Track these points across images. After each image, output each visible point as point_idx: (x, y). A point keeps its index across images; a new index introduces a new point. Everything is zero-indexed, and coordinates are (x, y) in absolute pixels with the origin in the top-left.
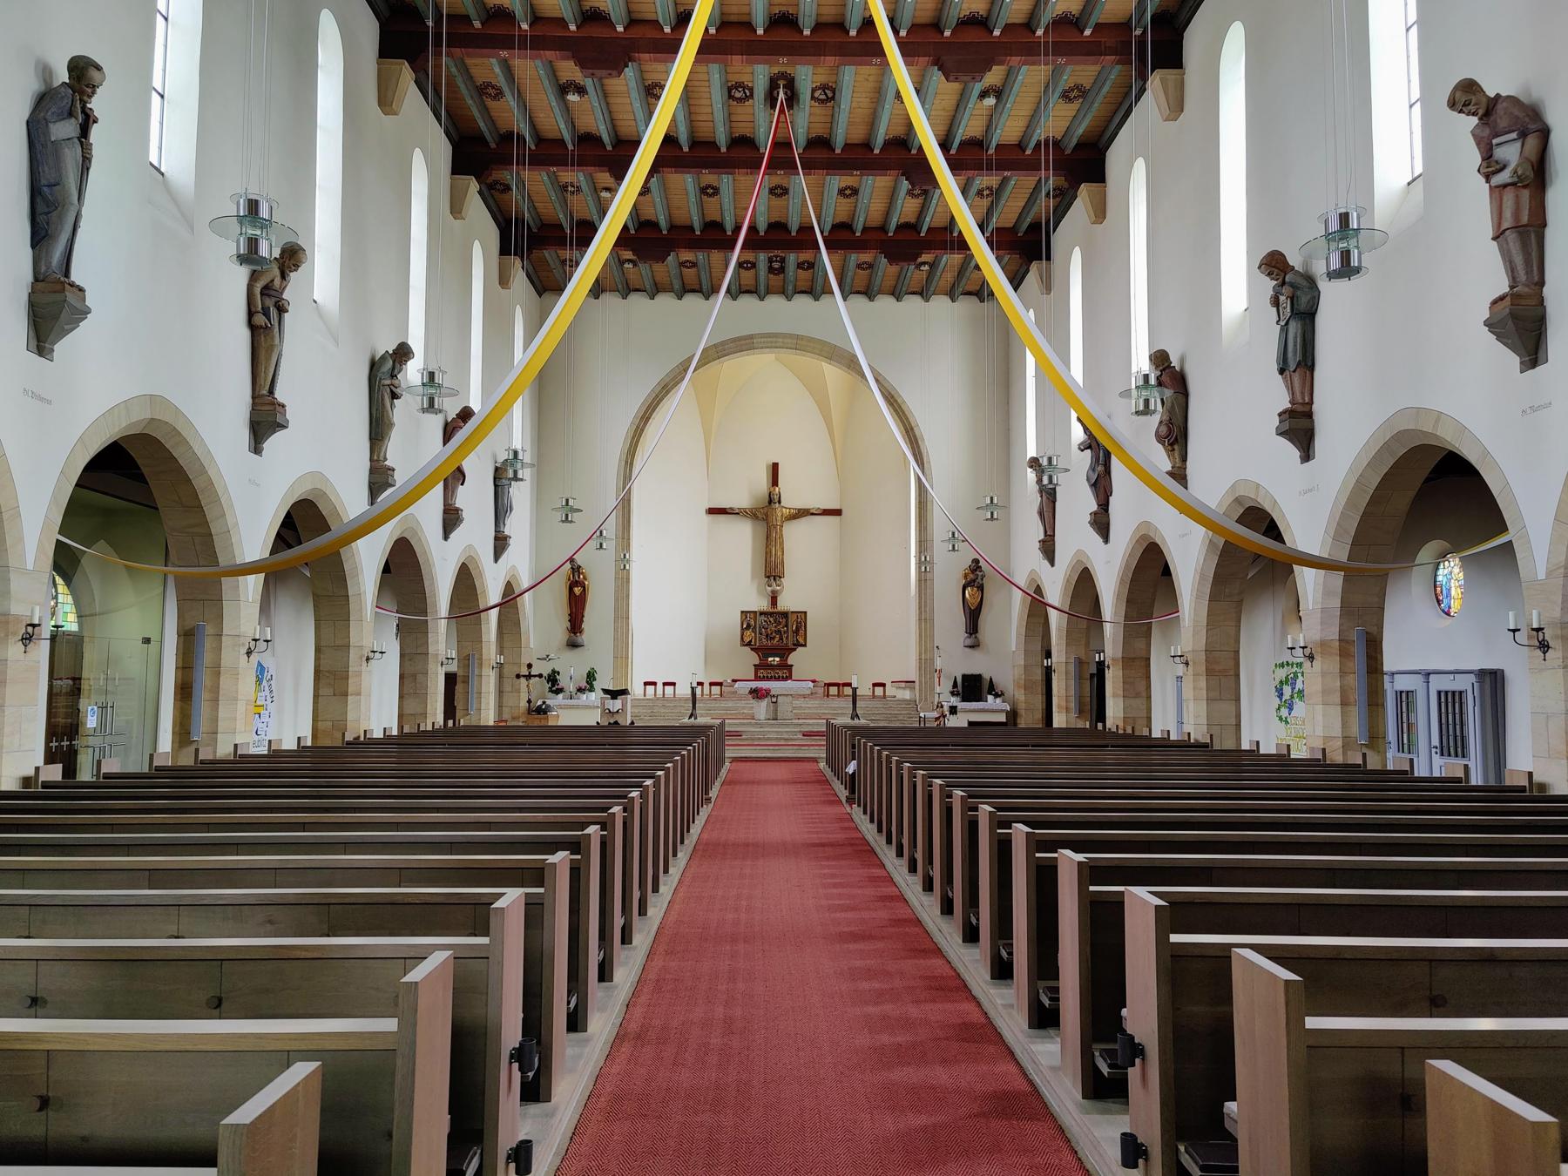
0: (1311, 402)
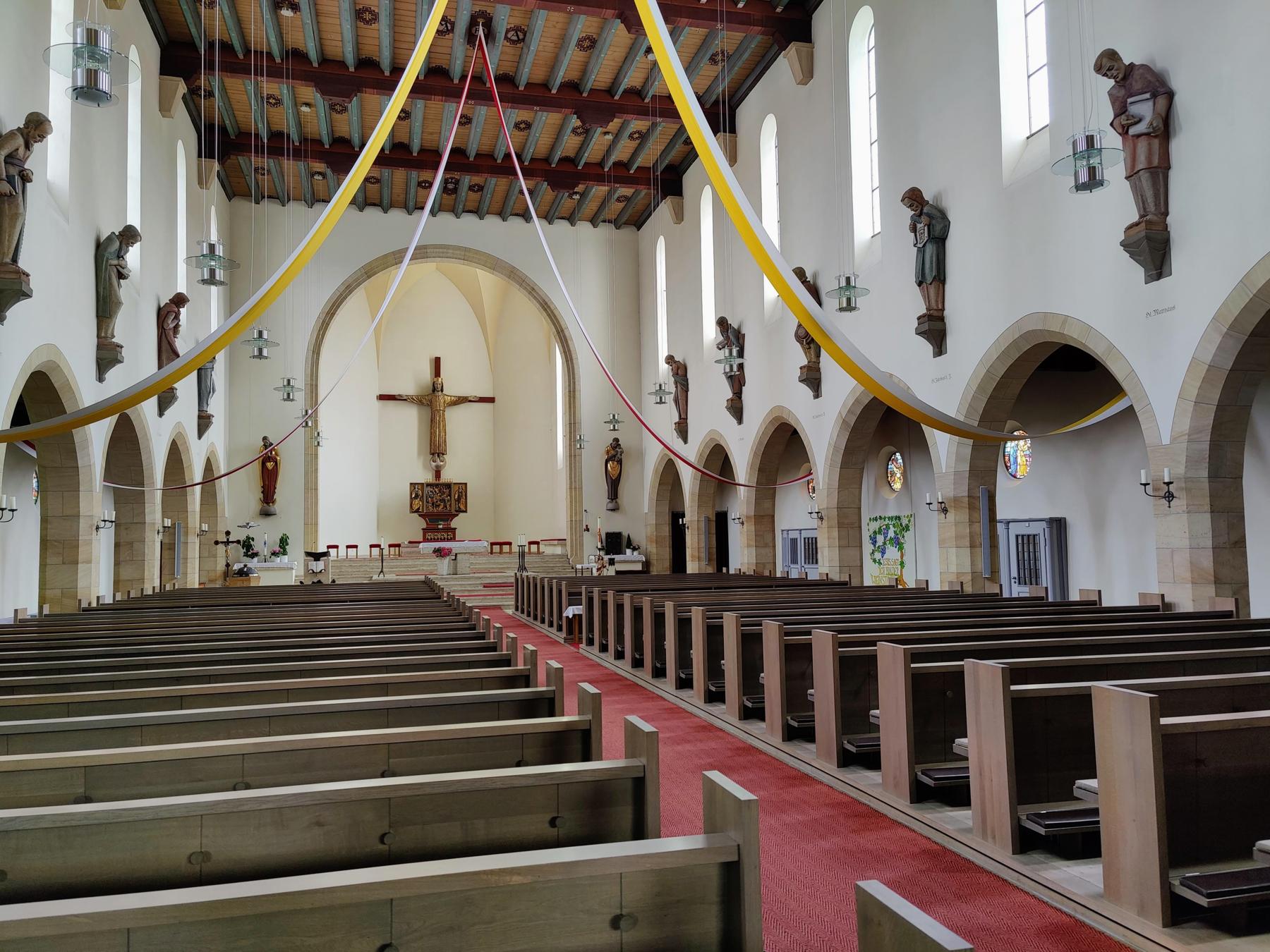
0: (943, 309)
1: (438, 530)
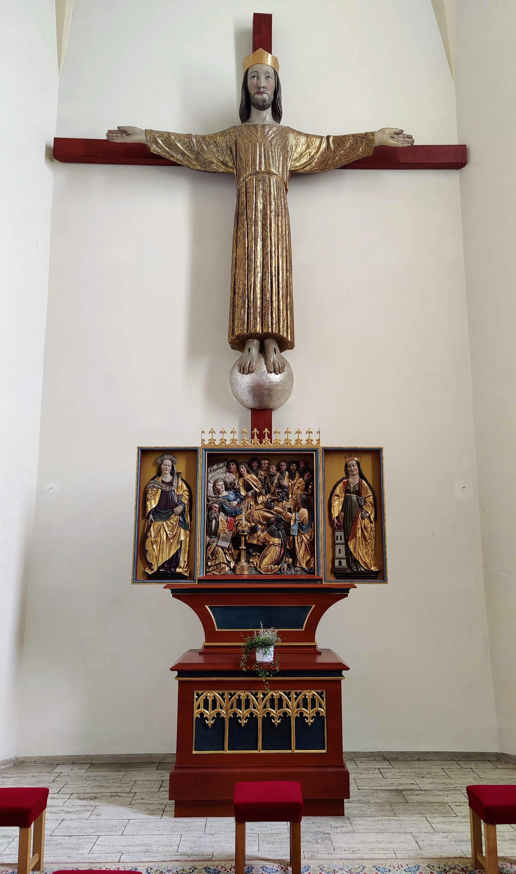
1: (251, 676)
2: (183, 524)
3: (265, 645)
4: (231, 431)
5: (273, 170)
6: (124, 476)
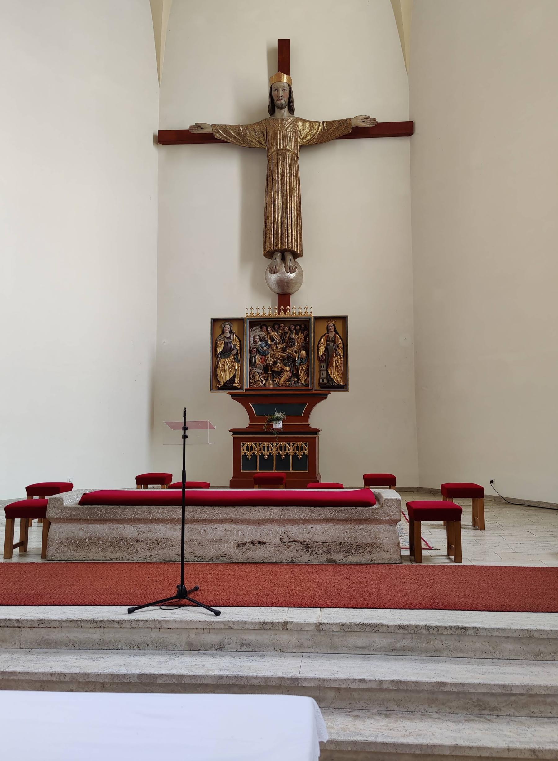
2: (236, 360)
3: (277, 419)
4: (265, 307)
5: (288, 148)
6: (204, 335)
